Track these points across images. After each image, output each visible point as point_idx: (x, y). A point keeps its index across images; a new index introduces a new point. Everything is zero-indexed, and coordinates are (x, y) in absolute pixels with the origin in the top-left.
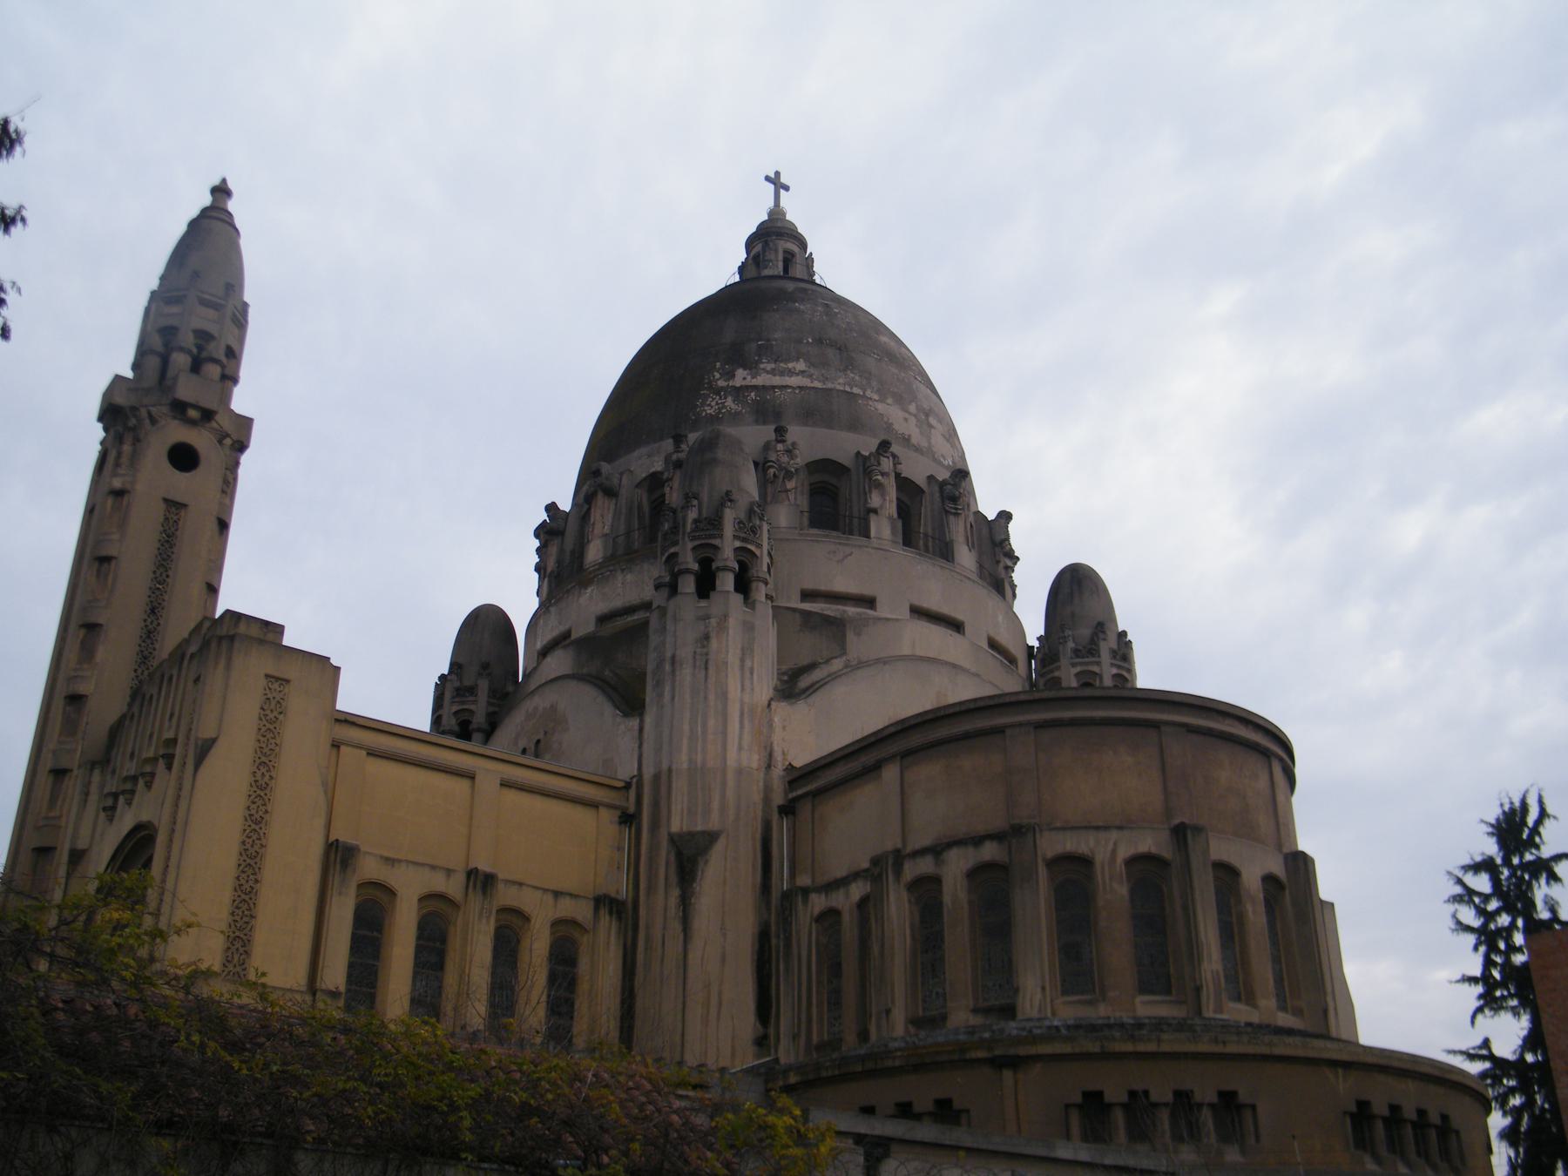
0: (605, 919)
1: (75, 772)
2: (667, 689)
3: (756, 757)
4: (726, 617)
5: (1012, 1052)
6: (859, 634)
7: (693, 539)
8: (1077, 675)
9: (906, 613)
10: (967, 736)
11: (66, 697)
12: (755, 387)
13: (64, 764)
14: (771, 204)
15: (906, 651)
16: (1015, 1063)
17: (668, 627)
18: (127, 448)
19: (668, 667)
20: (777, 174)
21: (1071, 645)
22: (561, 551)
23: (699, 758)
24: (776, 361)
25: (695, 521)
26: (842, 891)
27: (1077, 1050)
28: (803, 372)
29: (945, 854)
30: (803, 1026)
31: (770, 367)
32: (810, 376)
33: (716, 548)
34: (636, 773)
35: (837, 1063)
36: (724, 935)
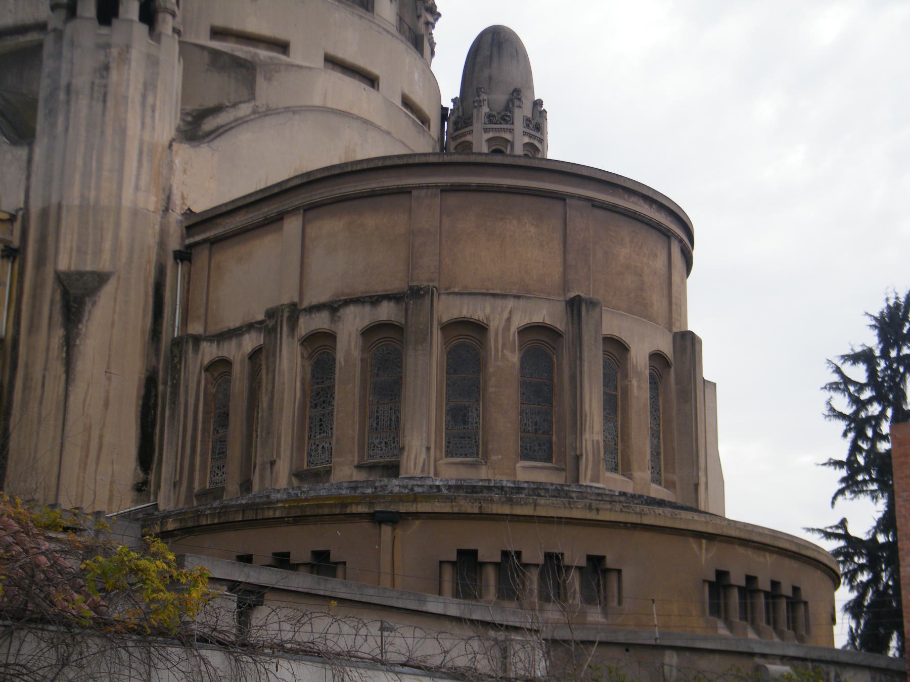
2: (61, 119)
3: (153, 199)
4: (128, 47)
5: (392, 508)
6: (269, 79)
8: (489, 141)
9: (320, 63)
10: (373, 194)
15: (317, 101)
16: (394, 519)
19: (62, 96)
21: (485, 109)
23: (93, 194)
26: (234, 342)
27: (456, 510)
29: (342, 311)
30: (186, 472)
35: (218, 511)
36: (109, 379)
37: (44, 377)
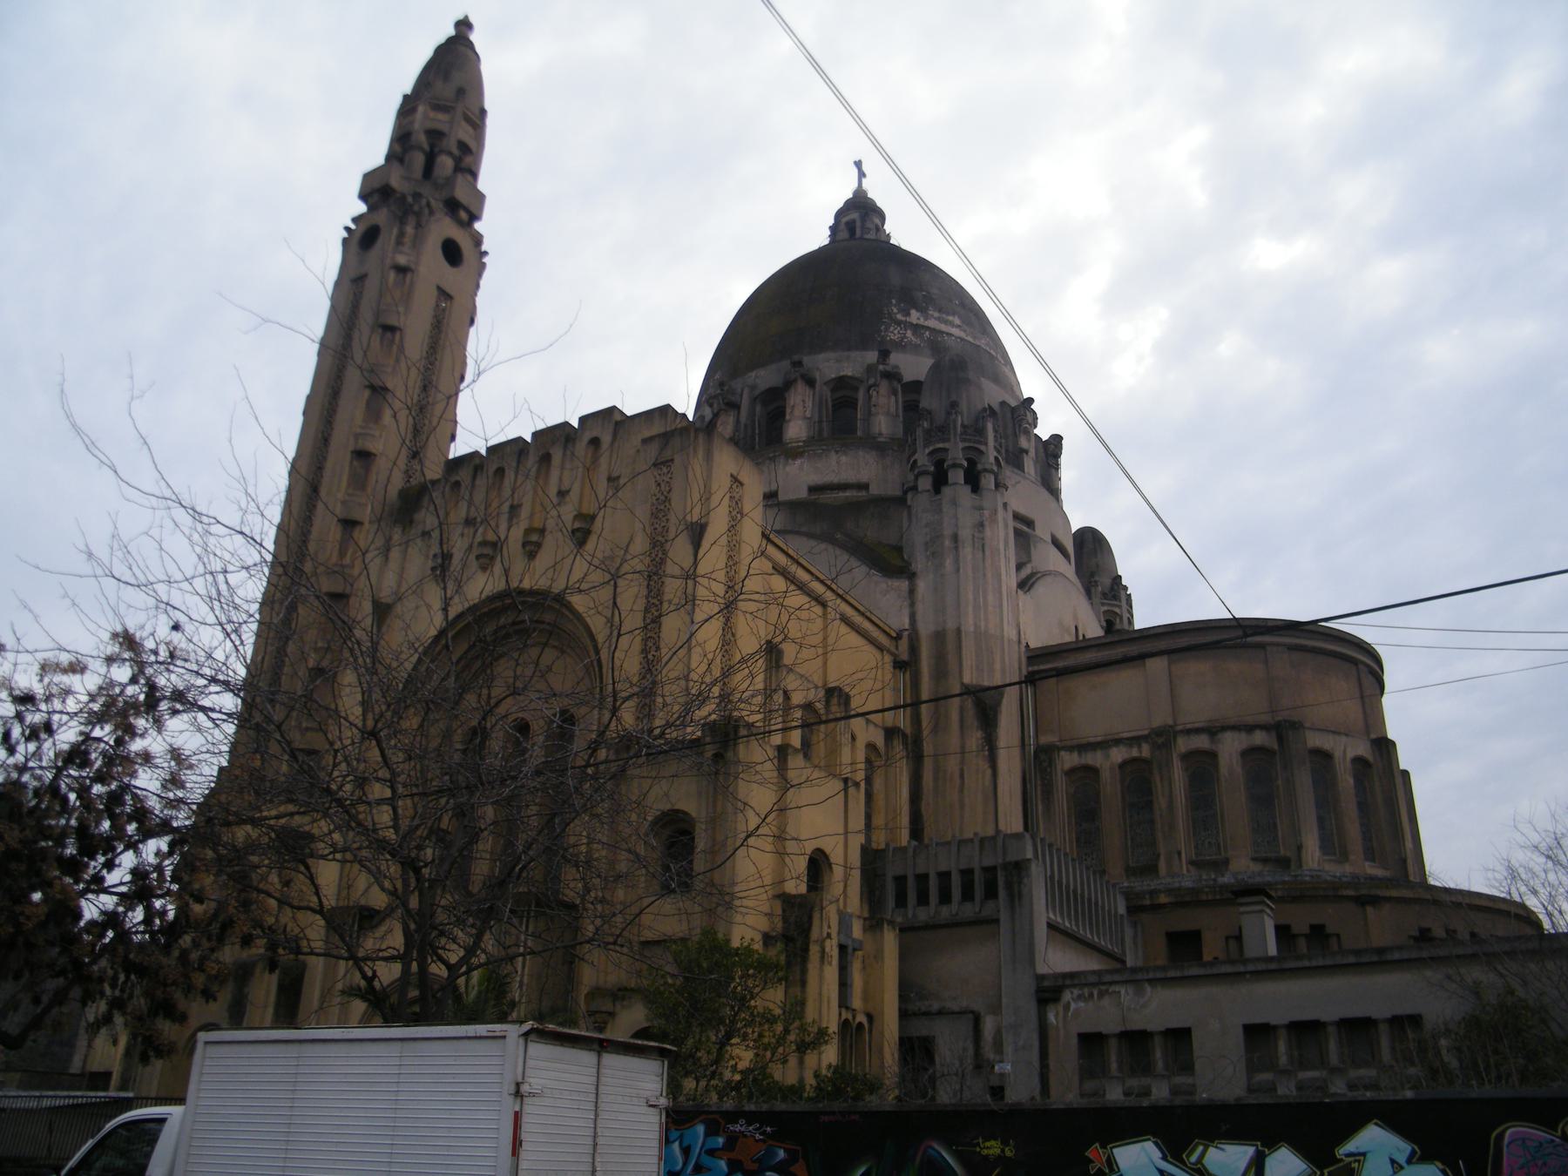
0: (898, 748)
1: (367, 525)
2: (949, 563)
4: (995, 512)
6: (1035, 547)
7: (964, 440)
8: (1105, 612)
11: (352, 452)
12: (928, 328)
13: (356, 516)
14: (855, 185)
17: (945, 510)
18: (409, 230)
19: (947, 543)
20: (860, 161)
21: (1100, 589)
22: (738, 422)
23: (983, 624)
24: (940, 311)
25: (963, 426)
26: (1099, 754)
27: (1417, 896)
28: (959, 326)
29: (1220, 736)
31: (936, 314)
32: (965, 331)
33: (981, 452)
34: (907, 627)
37: (962, 771)
